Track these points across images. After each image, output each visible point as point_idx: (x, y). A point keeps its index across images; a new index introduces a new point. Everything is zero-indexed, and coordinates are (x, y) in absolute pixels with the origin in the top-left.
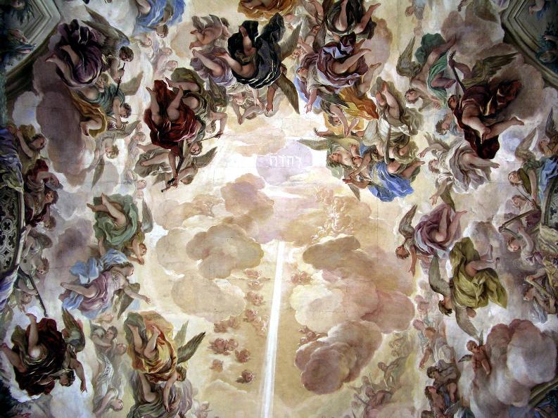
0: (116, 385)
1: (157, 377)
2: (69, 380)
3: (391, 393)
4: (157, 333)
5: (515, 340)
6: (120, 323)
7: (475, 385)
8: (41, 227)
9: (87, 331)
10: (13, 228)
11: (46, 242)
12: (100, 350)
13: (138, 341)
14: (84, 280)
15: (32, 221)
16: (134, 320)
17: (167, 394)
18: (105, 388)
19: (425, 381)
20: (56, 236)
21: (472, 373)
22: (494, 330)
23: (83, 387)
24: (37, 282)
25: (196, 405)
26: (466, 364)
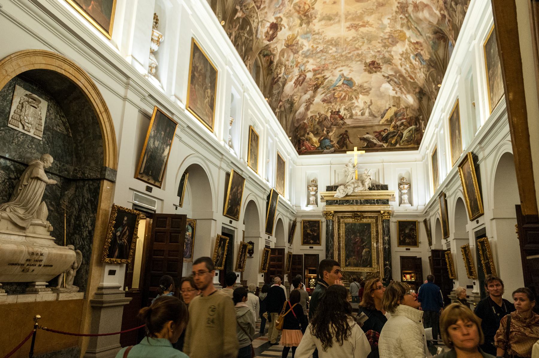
0: (294, 21)
1: (305, 13)
2: (281, 29)
3: (385, 4)
4: (303, 3)
5: (427, 8)
6: (291, 8)
7: (413, 11)
8: (262, 6)
9: (282, 16)
10: (255, 15)
11: (265, 8)
12: (287, 17)
13: (298, 8)
14: (278, 6)
15: (258, 8)
16: (296, 4)
17: (309, 15)
18: (291, 24)
19: (396, 4)
20: (267, 4)
21: (412, 8)
22: (421, 2)
23: (285, 28)
24: (265, 19)
25: (319, 13)
26: (411, 5)
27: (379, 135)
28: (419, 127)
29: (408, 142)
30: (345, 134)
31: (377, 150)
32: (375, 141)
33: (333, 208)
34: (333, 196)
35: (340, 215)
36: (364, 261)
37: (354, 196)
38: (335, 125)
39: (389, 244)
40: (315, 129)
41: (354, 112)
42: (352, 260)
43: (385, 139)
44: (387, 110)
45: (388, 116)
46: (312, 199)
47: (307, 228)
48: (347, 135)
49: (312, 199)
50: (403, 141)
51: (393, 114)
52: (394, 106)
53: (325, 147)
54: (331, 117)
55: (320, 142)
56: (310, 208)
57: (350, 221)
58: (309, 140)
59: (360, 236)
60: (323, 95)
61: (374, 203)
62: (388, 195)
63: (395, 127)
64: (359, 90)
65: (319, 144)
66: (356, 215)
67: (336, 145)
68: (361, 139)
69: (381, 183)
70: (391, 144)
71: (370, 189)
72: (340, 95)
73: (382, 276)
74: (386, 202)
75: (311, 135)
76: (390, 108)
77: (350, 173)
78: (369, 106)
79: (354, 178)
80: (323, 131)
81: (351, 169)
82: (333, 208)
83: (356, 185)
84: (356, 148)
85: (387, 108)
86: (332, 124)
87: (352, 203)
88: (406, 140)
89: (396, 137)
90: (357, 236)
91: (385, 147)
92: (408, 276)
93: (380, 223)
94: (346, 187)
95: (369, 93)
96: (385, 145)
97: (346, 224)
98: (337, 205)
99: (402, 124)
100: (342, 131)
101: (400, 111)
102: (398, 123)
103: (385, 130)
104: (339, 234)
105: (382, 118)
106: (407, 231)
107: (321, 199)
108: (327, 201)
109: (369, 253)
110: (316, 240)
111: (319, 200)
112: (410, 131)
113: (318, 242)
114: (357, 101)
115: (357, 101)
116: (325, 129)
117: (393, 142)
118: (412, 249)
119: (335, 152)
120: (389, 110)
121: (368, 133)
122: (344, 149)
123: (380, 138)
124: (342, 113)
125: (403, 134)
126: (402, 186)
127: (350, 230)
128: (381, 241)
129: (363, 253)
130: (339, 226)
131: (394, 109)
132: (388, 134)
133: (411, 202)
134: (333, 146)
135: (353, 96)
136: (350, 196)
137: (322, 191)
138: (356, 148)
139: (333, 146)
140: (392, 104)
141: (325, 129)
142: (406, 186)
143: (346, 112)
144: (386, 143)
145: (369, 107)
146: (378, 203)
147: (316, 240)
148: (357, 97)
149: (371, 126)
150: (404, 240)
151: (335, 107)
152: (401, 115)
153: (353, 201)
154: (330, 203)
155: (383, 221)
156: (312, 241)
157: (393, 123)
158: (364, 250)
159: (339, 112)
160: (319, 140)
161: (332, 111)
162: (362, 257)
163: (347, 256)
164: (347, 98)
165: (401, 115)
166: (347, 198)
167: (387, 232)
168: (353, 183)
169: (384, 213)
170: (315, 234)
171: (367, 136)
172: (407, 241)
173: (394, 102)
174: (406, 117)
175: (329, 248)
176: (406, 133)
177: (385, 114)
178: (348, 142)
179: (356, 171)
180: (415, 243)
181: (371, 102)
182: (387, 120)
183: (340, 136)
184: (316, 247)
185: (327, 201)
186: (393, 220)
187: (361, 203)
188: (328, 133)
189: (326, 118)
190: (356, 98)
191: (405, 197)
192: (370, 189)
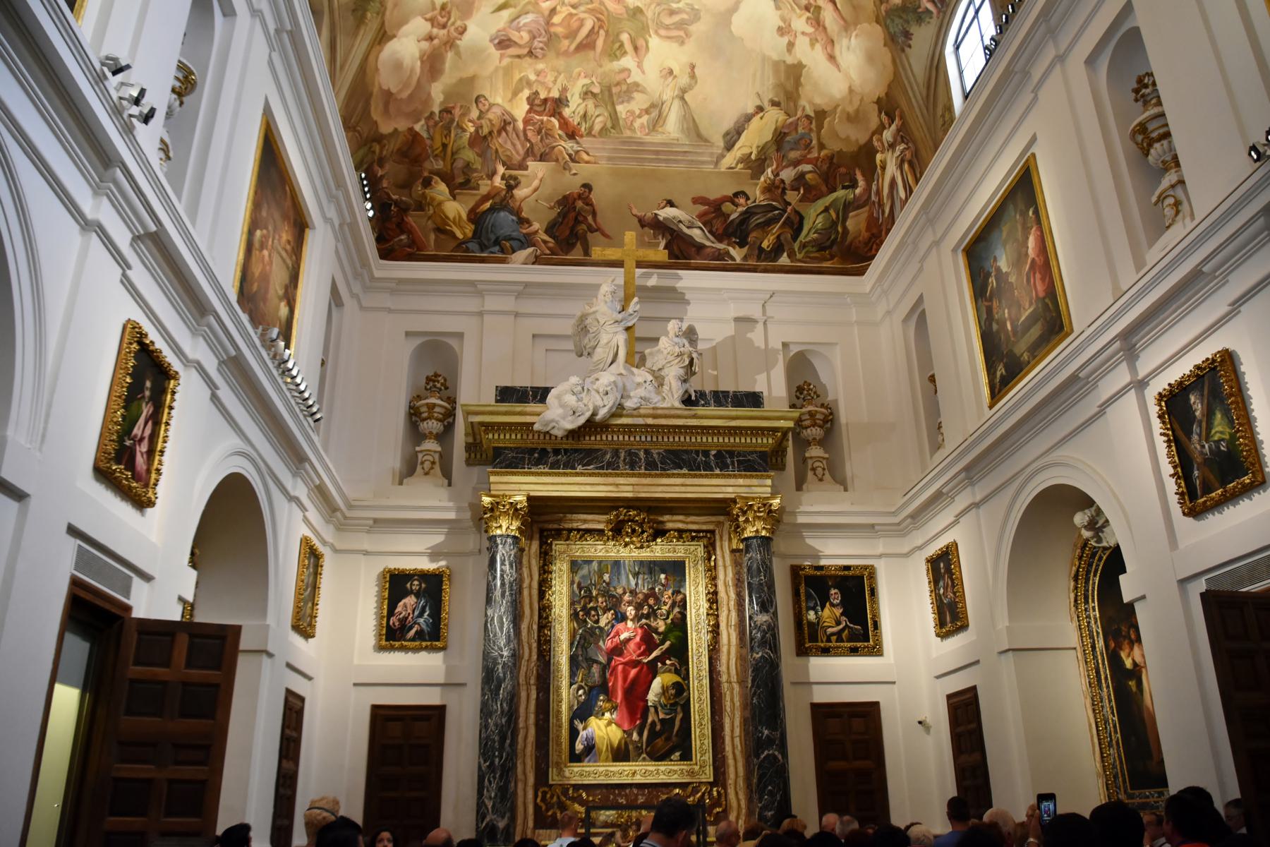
27: (713, 212)
28: (868, 189)
29: (822, 248)
30: (580, 196)
32: (696, 234)
36: (653, 735)
38: (542, 158)
40: (459, 164)
41: (621, 109)
43: (737, 232)
44: (748, 118)
45: (750, 142)
48: (589, 203)
50: (804, 246)
51: (768, 136)
52: (775, 104)
53: (497, 242)
54: (527, 122)
59: (638, 618)
60: (506, 14)
61: (708, 467)
64: (649, 14)
65: (469, 229)
68: (642, 223)
70: (761, 249)
72: (575, 25)
75: (441, 189)
76: (760, 109)
78: (684, 91)
80: (491, 175)
85: (751, 110)
86: (530, 153)
87: (610, 465)
88: (814, 240)
89: (776, 228)
91: (738, 260)
95: (688, 35)
96: (737, 254)
97: (575, 566)
98: (542, 469)
99: (801, 177)
100: (571, 184)
101: (795, 125)
102: (788, 175)
105: (729, 147)
107: (469, 448)
109: (680, 690)
112: (826, 210)
114: (640, 66)
115: (640, 66)
116: (501, 170)
117: (765, 244)
120: (756, 119)
121: (671, 204)
123: (718, 225)
124: (572, 111)
125: (802, 218)
129: (651, 697)
131: (774, 117)
132: (748, 214)
134: (527, 241)
135: (625, 37)
140: (769, 95)
141: (501, 170)
143: (590, 104)
144: (741, 245)
145: (682, 98)
146: (723, 466)
148: (641, 42)
151: (550, 78)
152: (797, 142)
153: (616, 453)
157: (769, 170)
158: (657, 684)
159: (560, 102)
160: (472, 212)
161: (537, 93)
164: (600, 43)
165: (796, 145)
166: (590, 442)
171: (667, 213)
173: (779, 86)
174: (814, 154)
176: (814, 218)
177: (739, 134)
181: (693, 76)
182: (746, 160)
187: (651, 465)
188: (510, 188)
189: (503, 128)
190: (636, 49)
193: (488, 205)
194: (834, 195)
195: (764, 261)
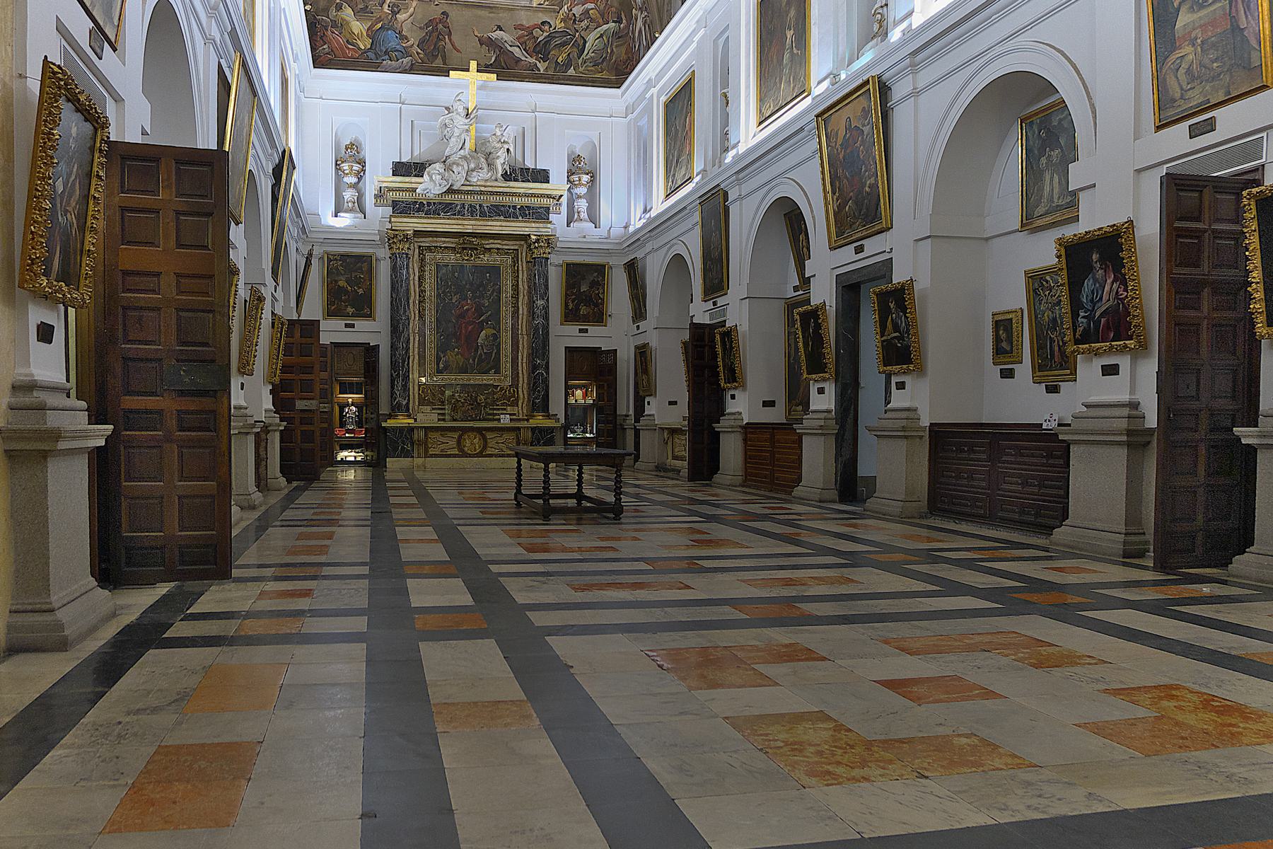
27: (526, 36)
28: (627, 27)
31: (521, 78)
32: (516, 51)
33: (412, 224)
34: (414, 190)
35: (426, 242)
36: (481, 361)
37: (468, 193)
39: (546, 318)
42: (452, 357)
43: (542, 50)
46: (349, 195)
47: (339, 274)
49: (349, 195)
53: (386, 53)
55: (372, 34)
56: (344, 221)
57: (451, 258)
58: (340, 25)
62: (549, 196)
63: (571, 19)
66: (467, 243)
67: (416, 49)
69: (529, 164)
71: (507, 177)
73: (523, 391)
74: (541, 214)
75: (348, 12)
77: (457, 132)
79: (467, 145)
81: (460, 121)
82: (412, 224)
83: (472, 166)
84: (473, 64)
90: (466, 299)
92: (579, 393)
93: (522, 266)
94: (449, 168)
96: (542, 66)
102: (578, 10)
103: (543, 23)
104: (422, 291)
106: (584, 288)
108: (395, 204)
110: (363, 306)
111: (369, 200)
112: (601, 36)
113: (367, 311)
118: (593, 330)
119: (411, 70)
122: (438, 62)
123: (530, 45)
125: (585, 42)
126: (575, 178)
127: (449, 282)
128: (523, 310)
130: (422, 269)
132: (551, 37)
133: (594, 219)
134: (406, 53)
136: (458, 192)
137: (379, 175)
138: (473, 64)
139: (406, 53)
142: (585, 178)
147: (363, 306)
149: (510, 10)
150: (578, 309)
154: (401, 208)
155: (533, 262)
156: (350, 310)
162: (476, 350)
163: (442, 348)
166: (448, 198)
167: (538, 288)
168: (464, 158)
169: (537, 241)
170: (361, 291)
171: (498, 34)
172: (583, 310)
175: (397, 328)
178: (449, 46)
179: (473, 129)
180: (599, 317)
183: (427, 25)
184: (360, 324)
185: (395, 204)
186: (555, 259)
187: (483, 214)
188: (394, 13)
191: (582, 205)
192: (507, 177)
193: (379, 25)
194: (605, 27)
195: (557, 76)
